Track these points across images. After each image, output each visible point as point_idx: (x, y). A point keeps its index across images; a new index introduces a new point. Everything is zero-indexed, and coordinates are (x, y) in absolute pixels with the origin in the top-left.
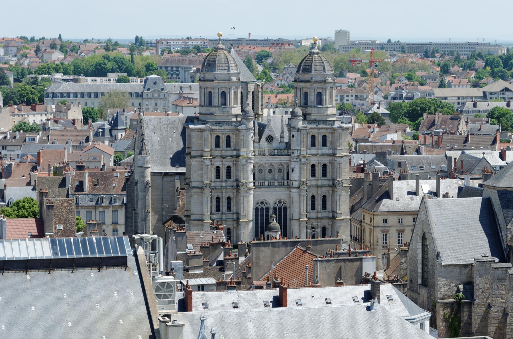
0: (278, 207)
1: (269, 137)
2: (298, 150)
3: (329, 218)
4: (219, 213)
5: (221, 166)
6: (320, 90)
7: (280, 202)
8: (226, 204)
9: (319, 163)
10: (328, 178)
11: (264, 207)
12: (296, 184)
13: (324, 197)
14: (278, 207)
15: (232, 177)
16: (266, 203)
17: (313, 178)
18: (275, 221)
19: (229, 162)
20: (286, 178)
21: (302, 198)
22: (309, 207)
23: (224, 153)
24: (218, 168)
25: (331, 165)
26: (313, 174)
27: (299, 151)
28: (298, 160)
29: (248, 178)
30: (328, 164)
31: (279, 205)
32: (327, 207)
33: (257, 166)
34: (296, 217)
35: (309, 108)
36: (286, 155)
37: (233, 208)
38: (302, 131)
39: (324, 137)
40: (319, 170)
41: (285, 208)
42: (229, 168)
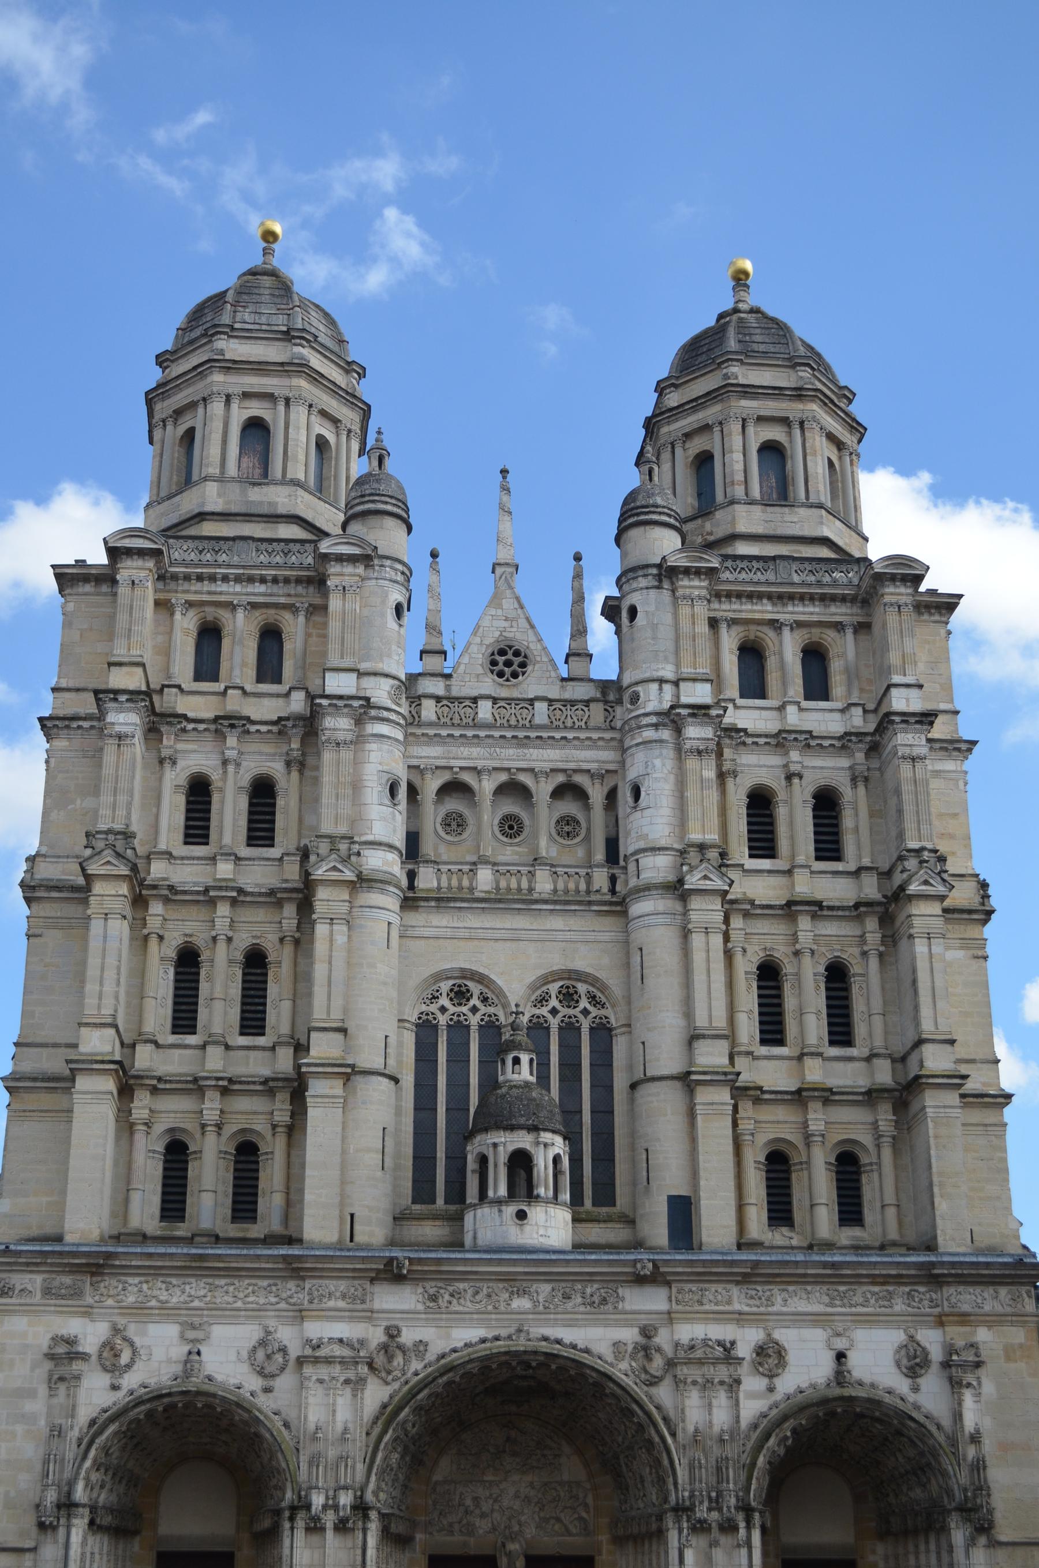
0: (554, 1023)
1: (502, 652)
2: (661, 681)
3: (871, 1096)
4: (191, 1040)
5: (215, 776)
6: (775, 433)
7: (569, 996)
8: (236, 990)
9: (789, 777)
10: (852, 867)
11: (474, 1020)
12: (657, 867)
13: (837, 976)
14: (554, 1023)
15: (277, 840)
16: (485, 1000)
17: (765, 864)
18: (525, 1074)
19: (262, 759)
20: (600, 856)
21: (697, 940)
22: (748, 1027)
23: (235, 703)
24: (199, 791)
25: (861, 789)
26: (763, 841)
27: (668, 688)
28: (666, 734)
29: (357, 819)
30: (847, 793)
31: (564, 1011)
32: (860, 1030)
33: (432, 785)
34: (667, 1059)
35: (719, 515)
36: (598, 729)
37: (278, 1015)
38: (684, 582)
39: (815, 657)
40: (796, 823)
41: (603, 1033)
42: (262, 792)
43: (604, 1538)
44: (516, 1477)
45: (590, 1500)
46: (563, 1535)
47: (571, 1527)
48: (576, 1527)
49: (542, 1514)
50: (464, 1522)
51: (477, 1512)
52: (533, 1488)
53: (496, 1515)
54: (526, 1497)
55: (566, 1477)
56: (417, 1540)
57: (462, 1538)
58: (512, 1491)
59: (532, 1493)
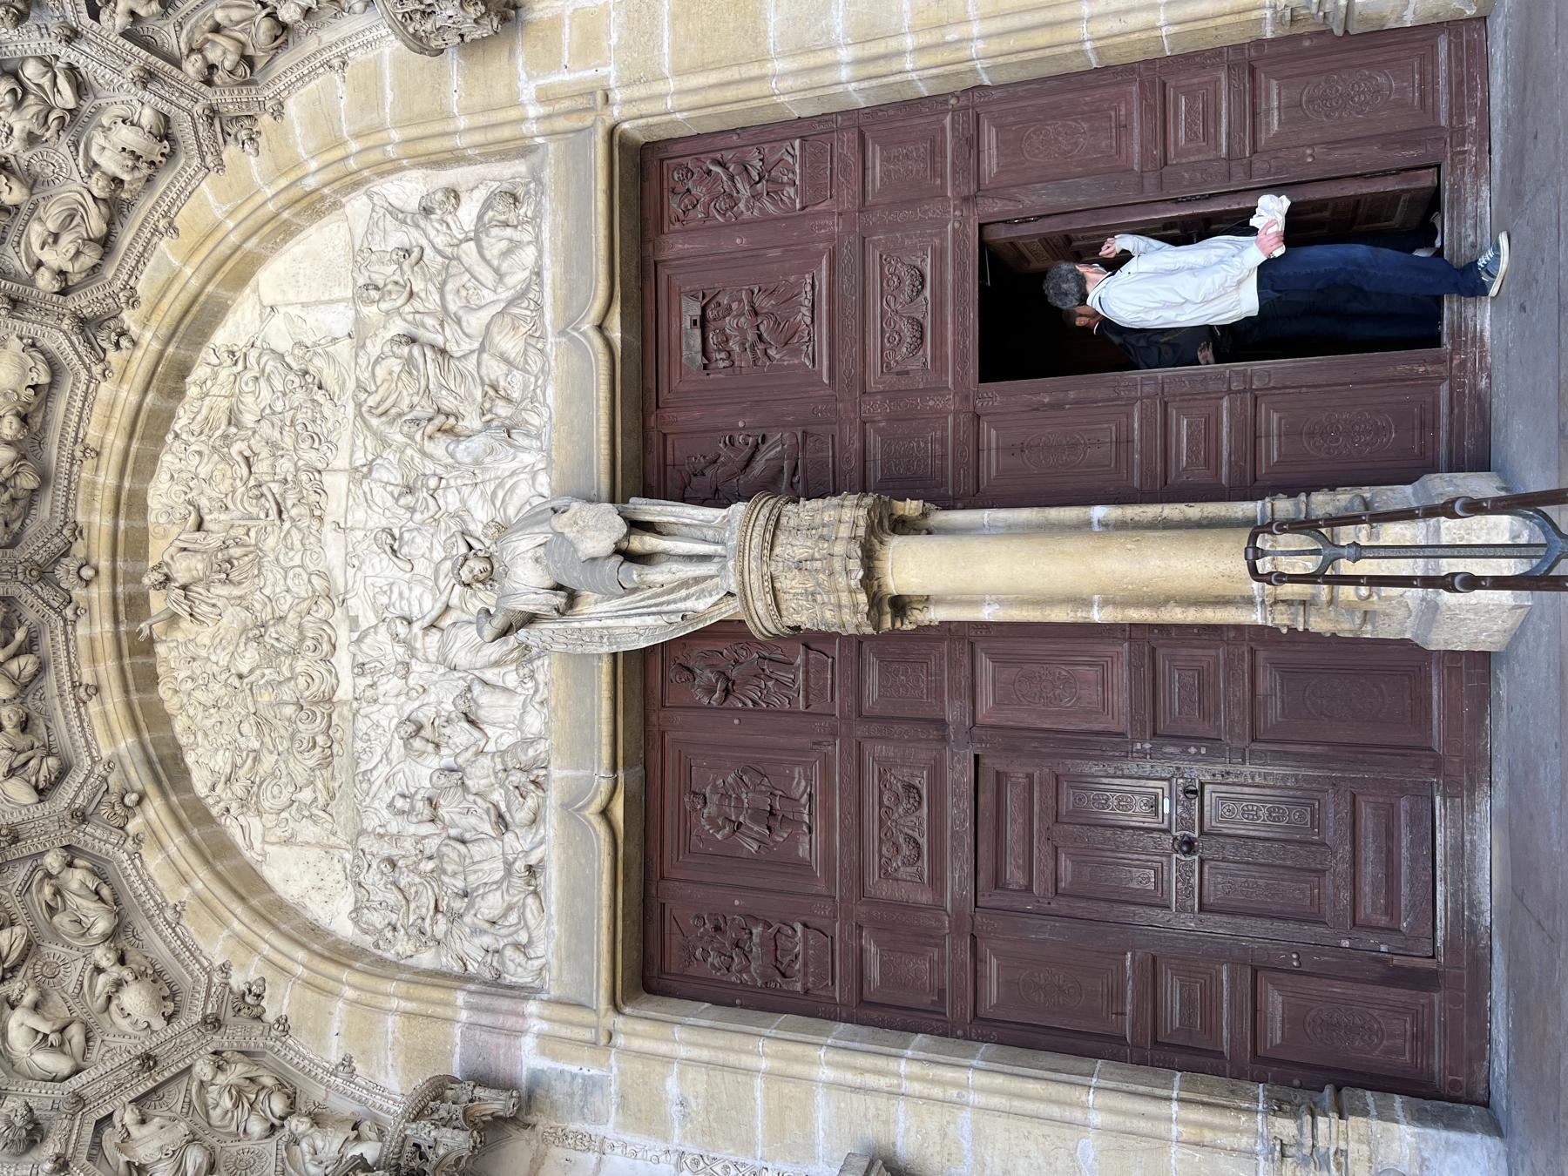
43: (524, 83)
44: (334, 554)
45: (408, 189)
46: (539, 307)
47: (517, 278)
48: (514, 247)
49: (472, 422)
50: (497, 796)
51: (461, 734)
52: (370, 465)
53: (461, 657)
54: (397, 500)
55: (339, 320)
56: (543, 1063)
57: (552, 826)
58: (381, 567)
59: (387, 473)
